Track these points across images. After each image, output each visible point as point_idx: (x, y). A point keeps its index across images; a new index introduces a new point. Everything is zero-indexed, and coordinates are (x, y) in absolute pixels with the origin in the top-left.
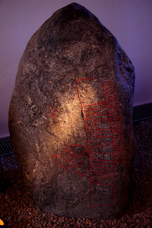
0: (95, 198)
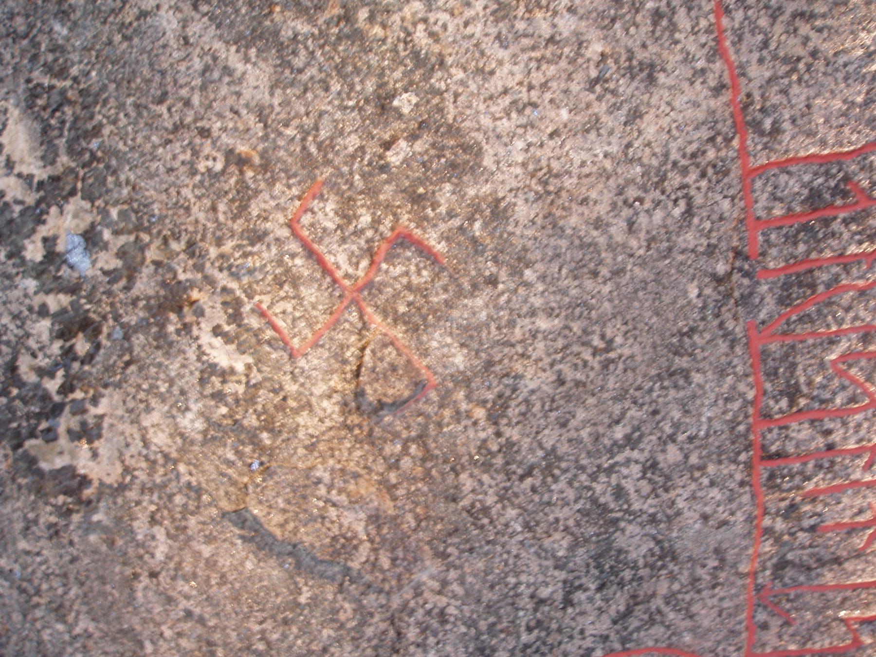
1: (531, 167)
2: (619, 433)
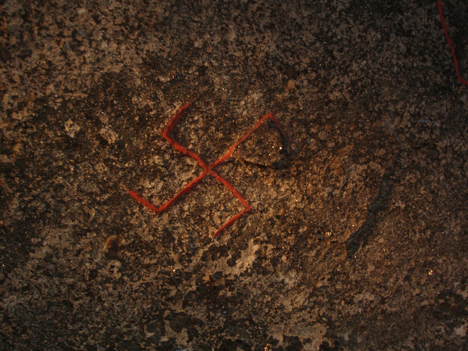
1: (121, 38)
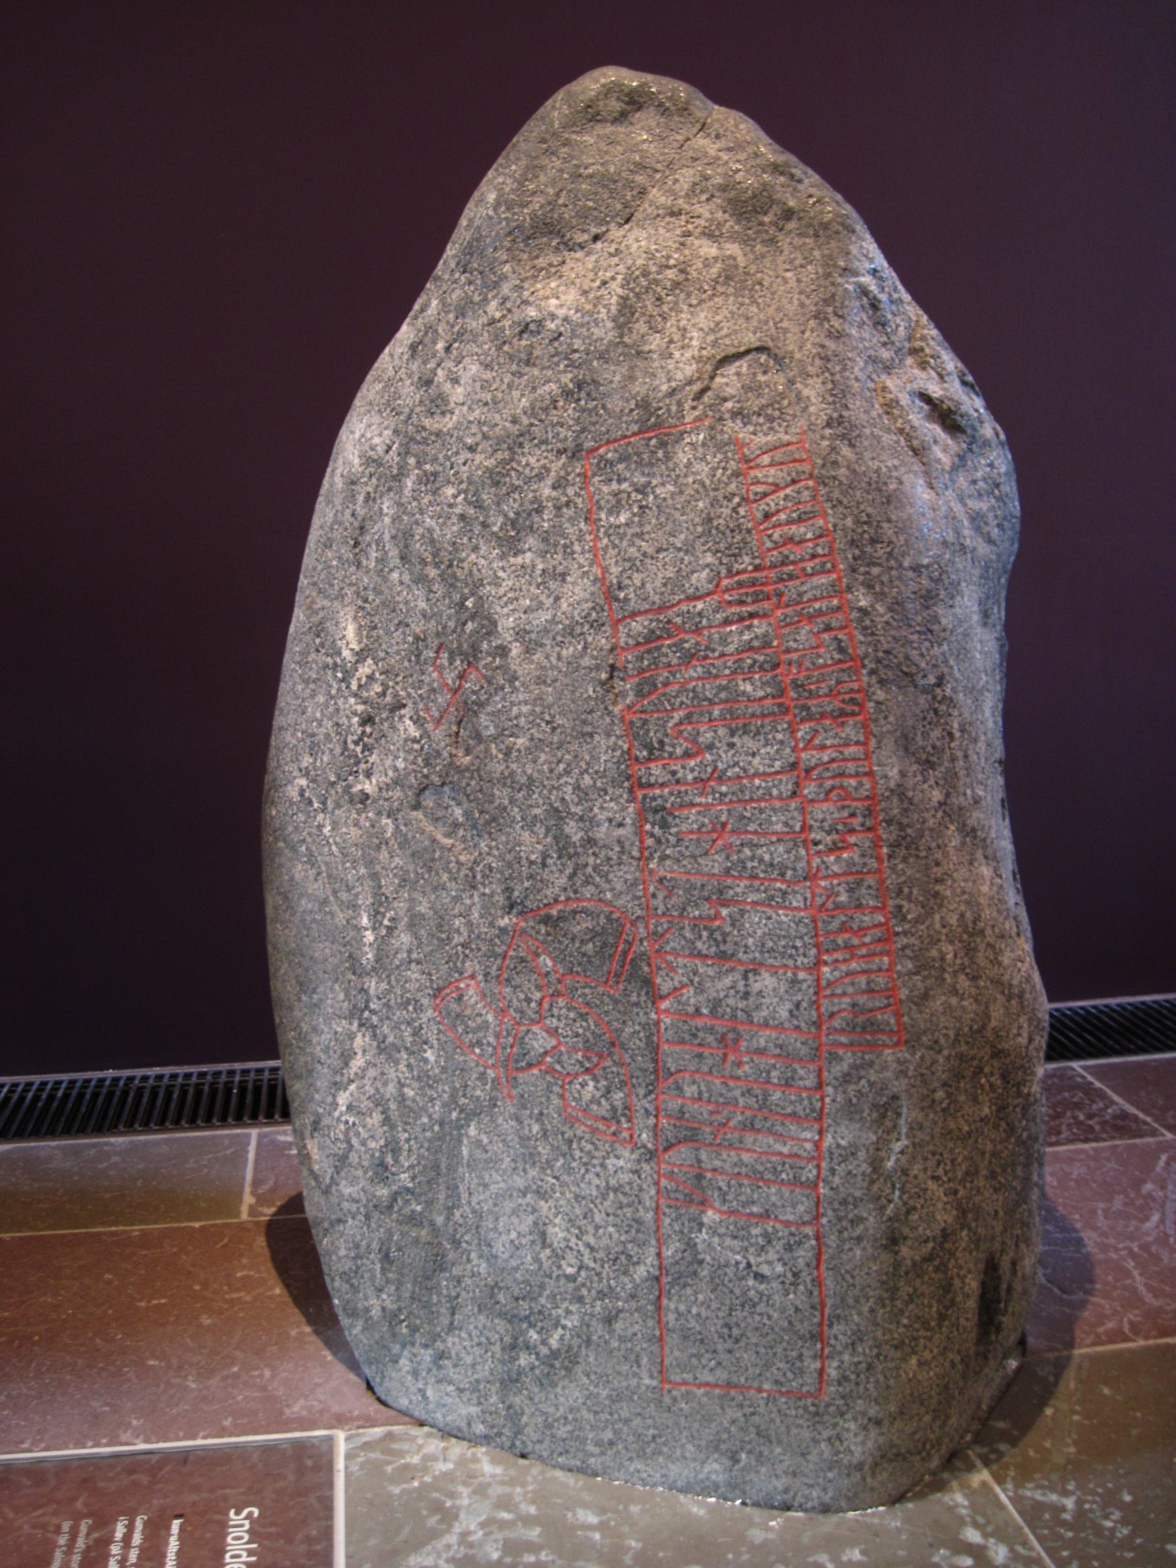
0: (693, 1323)
2: (562, 766)
